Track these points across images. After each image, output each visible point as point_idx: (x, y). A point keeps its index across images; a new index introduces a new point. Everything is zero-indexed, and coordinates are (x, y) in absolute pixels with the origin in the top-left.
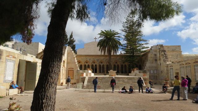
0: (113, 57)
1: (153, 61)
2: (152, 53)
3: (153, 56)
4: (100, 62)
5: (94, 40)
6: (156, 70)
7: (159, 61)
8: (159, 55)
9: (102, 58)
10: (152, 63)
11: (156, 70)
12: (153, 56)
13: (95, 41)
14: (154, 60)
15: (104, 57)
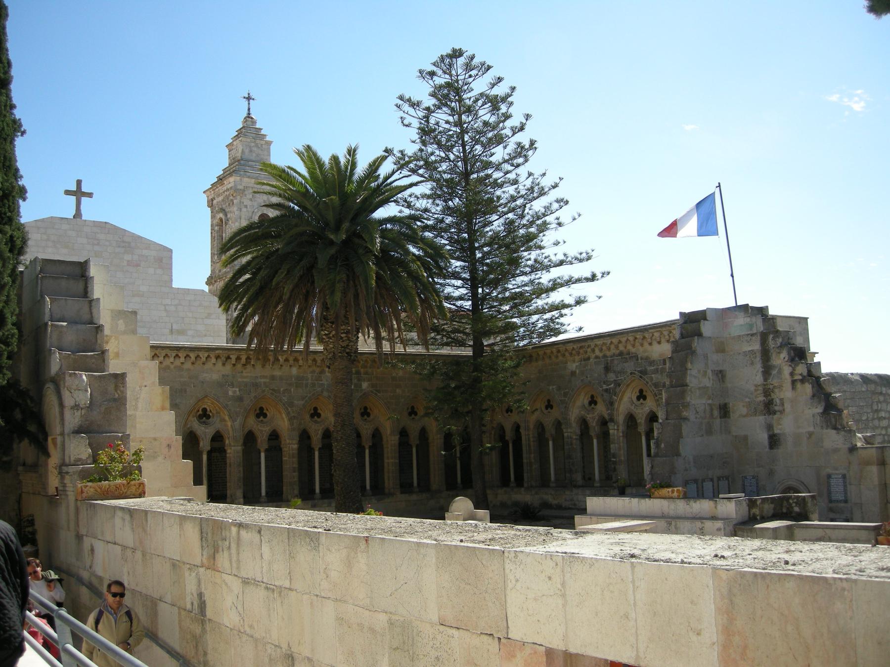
0: (294, 371)
1: (712, 415)
2: (706, 357)
3: (708, 382)
4: (191, 412)
5: (66, 208)
6: (727, 478)
7: (761, 418)
8: (759, 379)
9: (214, 372)
10: (709, 432)
11: (727, 478)
12: (709, 384)
13: (70, 213)
14: (716, 413)
15: (228, 369)
